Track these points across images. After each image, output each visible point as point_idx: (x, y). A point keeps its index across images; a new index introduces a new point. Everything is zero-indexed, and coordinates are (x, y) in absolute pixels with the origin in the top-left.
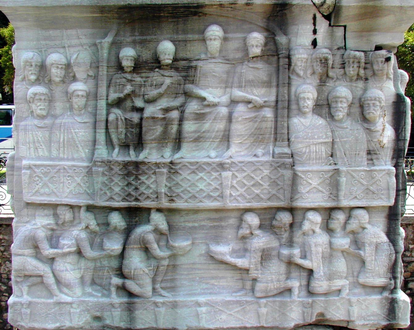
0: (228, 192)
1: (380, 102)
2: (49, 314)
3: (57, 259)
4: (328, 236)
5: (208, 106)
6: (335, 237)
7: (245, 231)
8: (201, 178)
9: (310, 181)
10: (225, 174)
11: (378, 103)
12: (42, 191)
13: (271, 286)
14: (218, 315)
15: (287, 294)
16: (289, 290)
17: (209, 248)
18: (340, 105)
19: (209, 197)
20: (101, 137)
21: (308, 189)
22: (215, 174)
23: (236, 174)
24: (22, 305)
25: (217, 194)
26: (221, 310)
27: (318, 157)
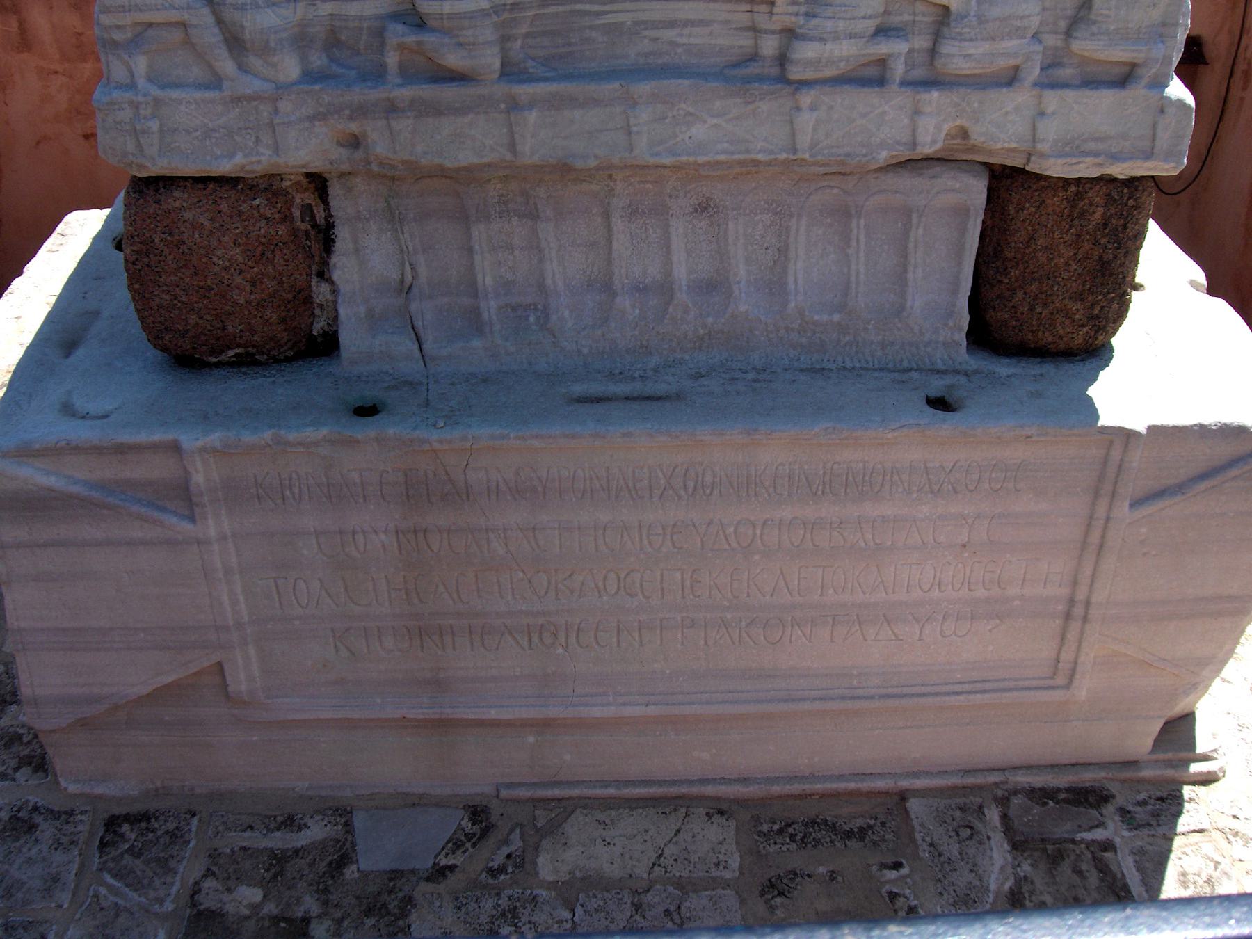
2: (214, 130)
14: (684, 129)
26: (691, 114)
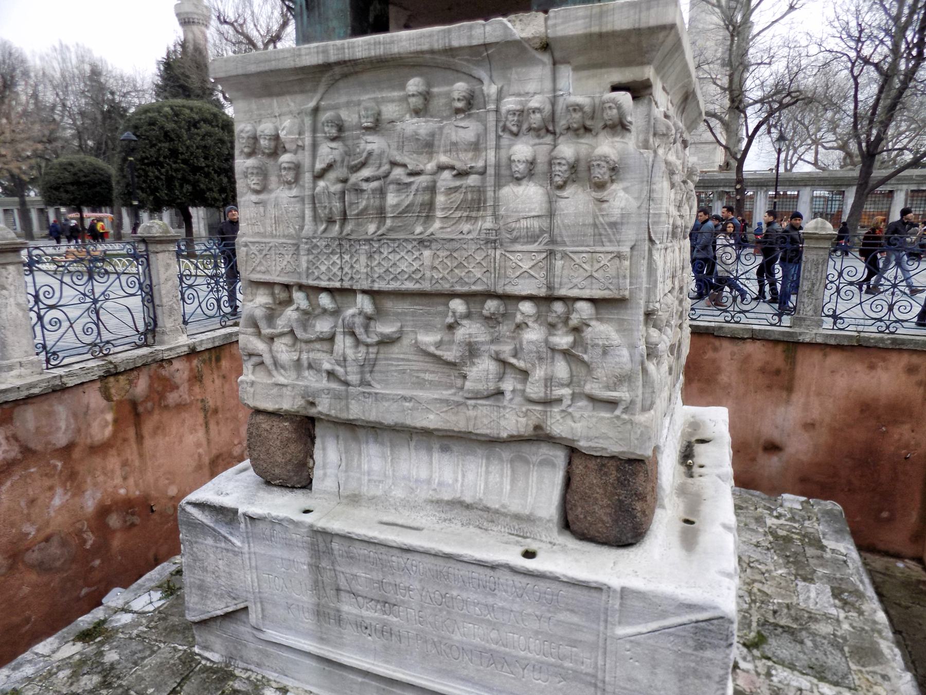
0: (428, 274)
1: (607, 162)
3: (275, 339)
4: (547, 331)
5: (411, 174)
6: (555, 335)
7: (450, 320)
8: (403, 257)
9: (520, 264)
10: (427, 253)
11: (603, 164)
12: (258, 269)
13: (480, 387)
15: (500, 397)
16: (500, 393)
18: (558, 168)
19: (410, 278)
20: (308, 213)
21: (518, 273)
22: (417, 254)
23: (438, 253)
25: (420, 276)
27: (530, 234)
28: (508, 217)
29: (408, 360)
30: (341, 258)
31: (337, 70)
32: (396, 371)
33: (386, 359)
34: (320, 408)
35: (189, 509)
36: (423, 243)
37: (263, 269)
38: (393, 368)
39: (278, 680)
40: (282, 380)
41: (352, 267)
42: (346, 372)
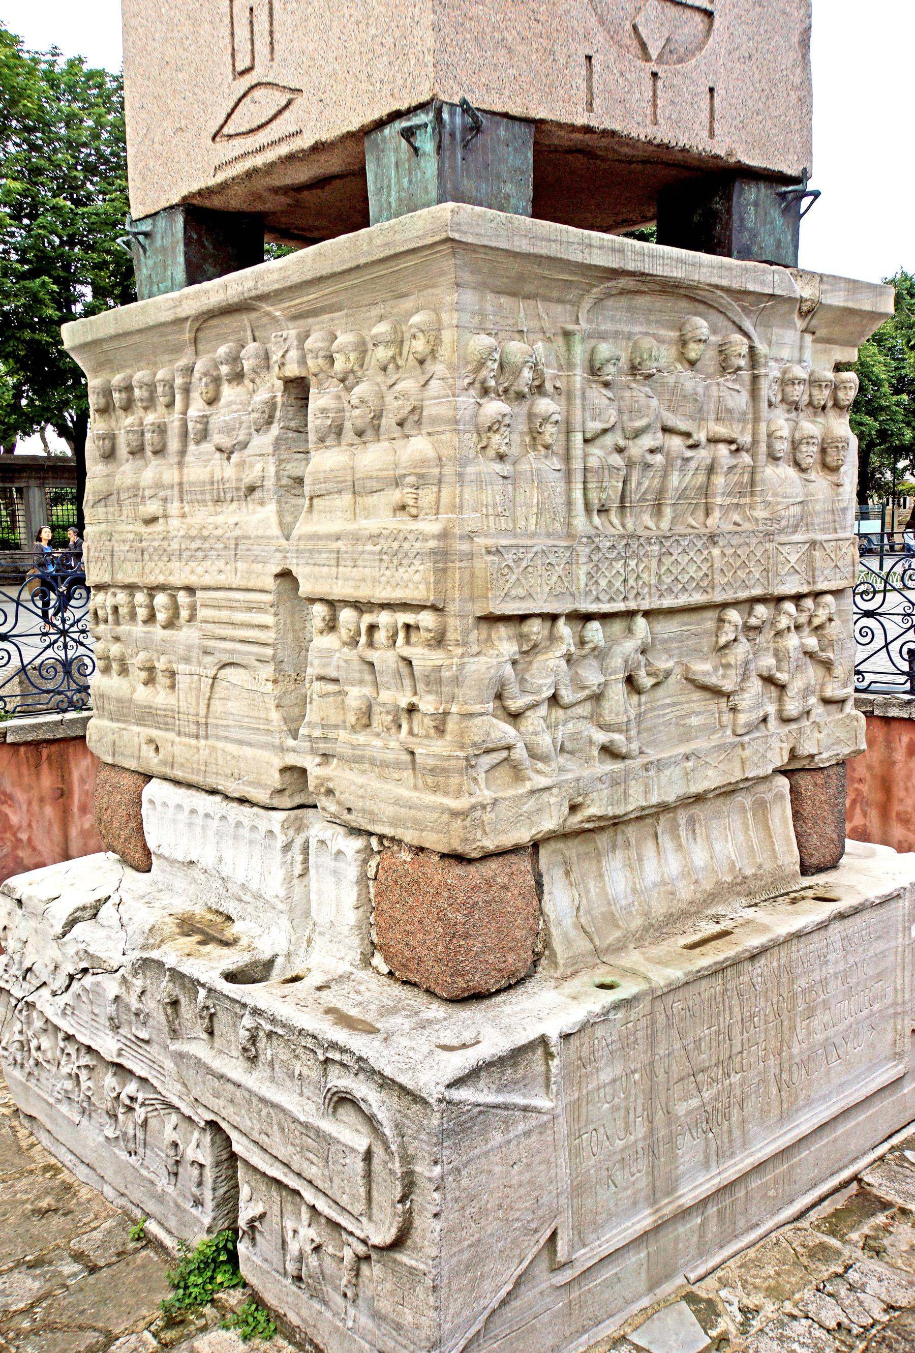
10: (716, 552)
12: (513, 593)
17: (687, 669)
24: (484, 807)
28: (778, 503)
29: (681, 703)
30: (626, 565)
31: (623, 282)
32: (664, 723)
33: (652, 709)
34: (593, 810)
35: (459, 1094)
36: (712, 539)
37: (521, 592)
38: (661, 720)
39: (592, 1342)
40: (542, 781)
41: (638, 577)
42: (628, 739)
